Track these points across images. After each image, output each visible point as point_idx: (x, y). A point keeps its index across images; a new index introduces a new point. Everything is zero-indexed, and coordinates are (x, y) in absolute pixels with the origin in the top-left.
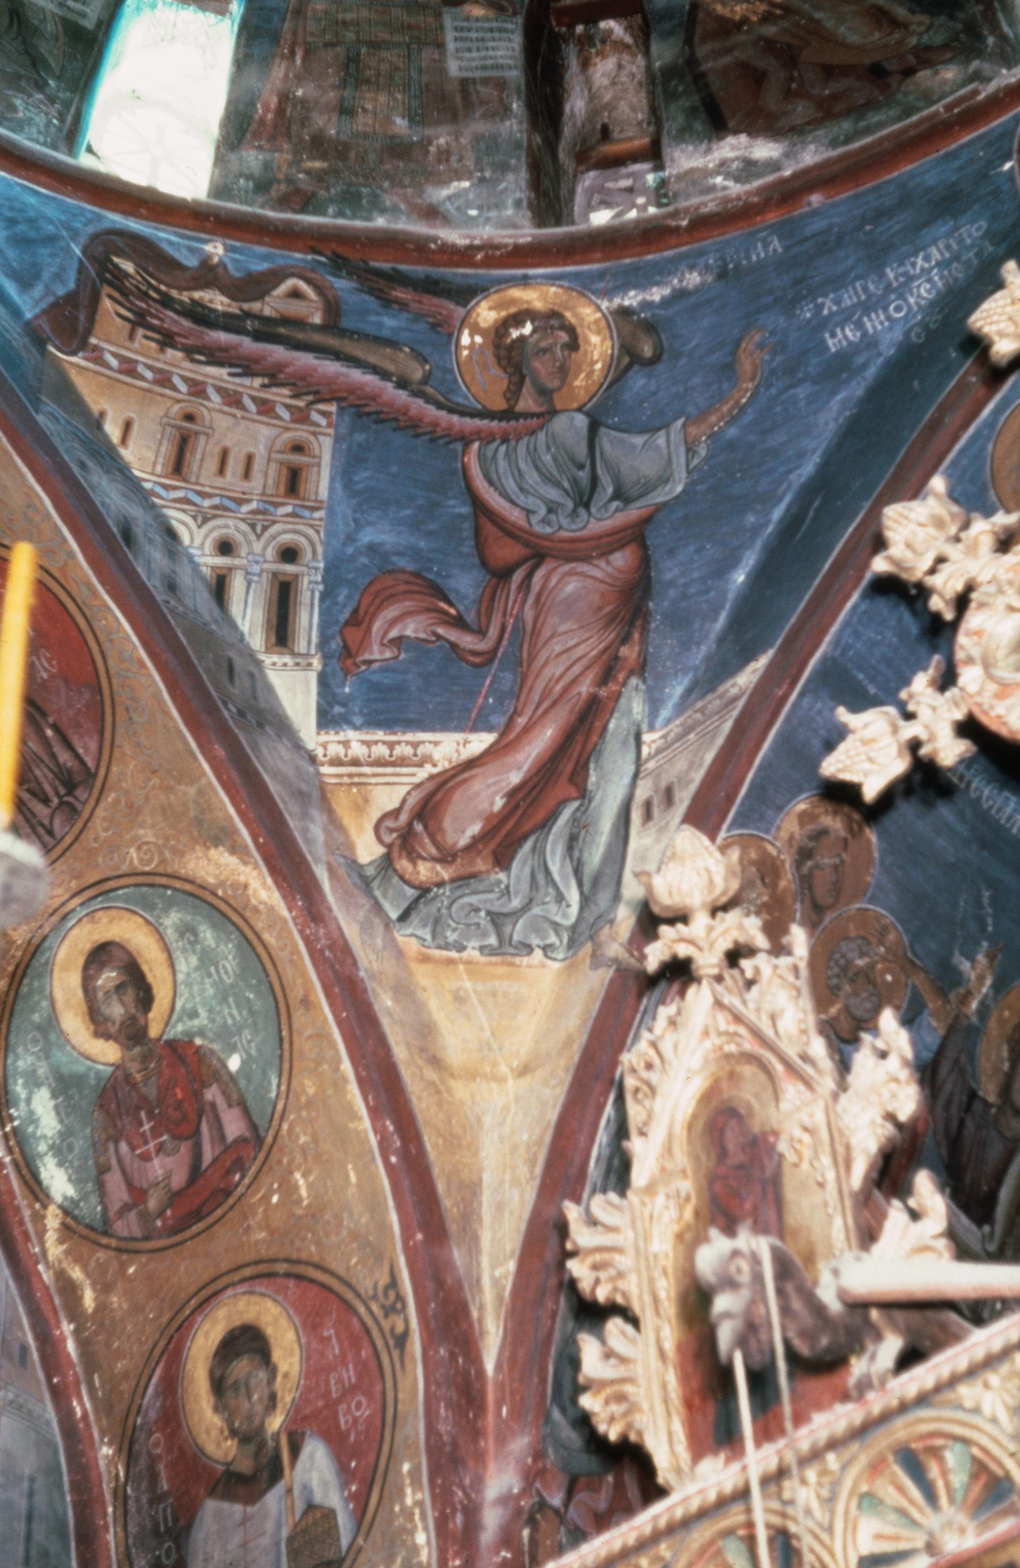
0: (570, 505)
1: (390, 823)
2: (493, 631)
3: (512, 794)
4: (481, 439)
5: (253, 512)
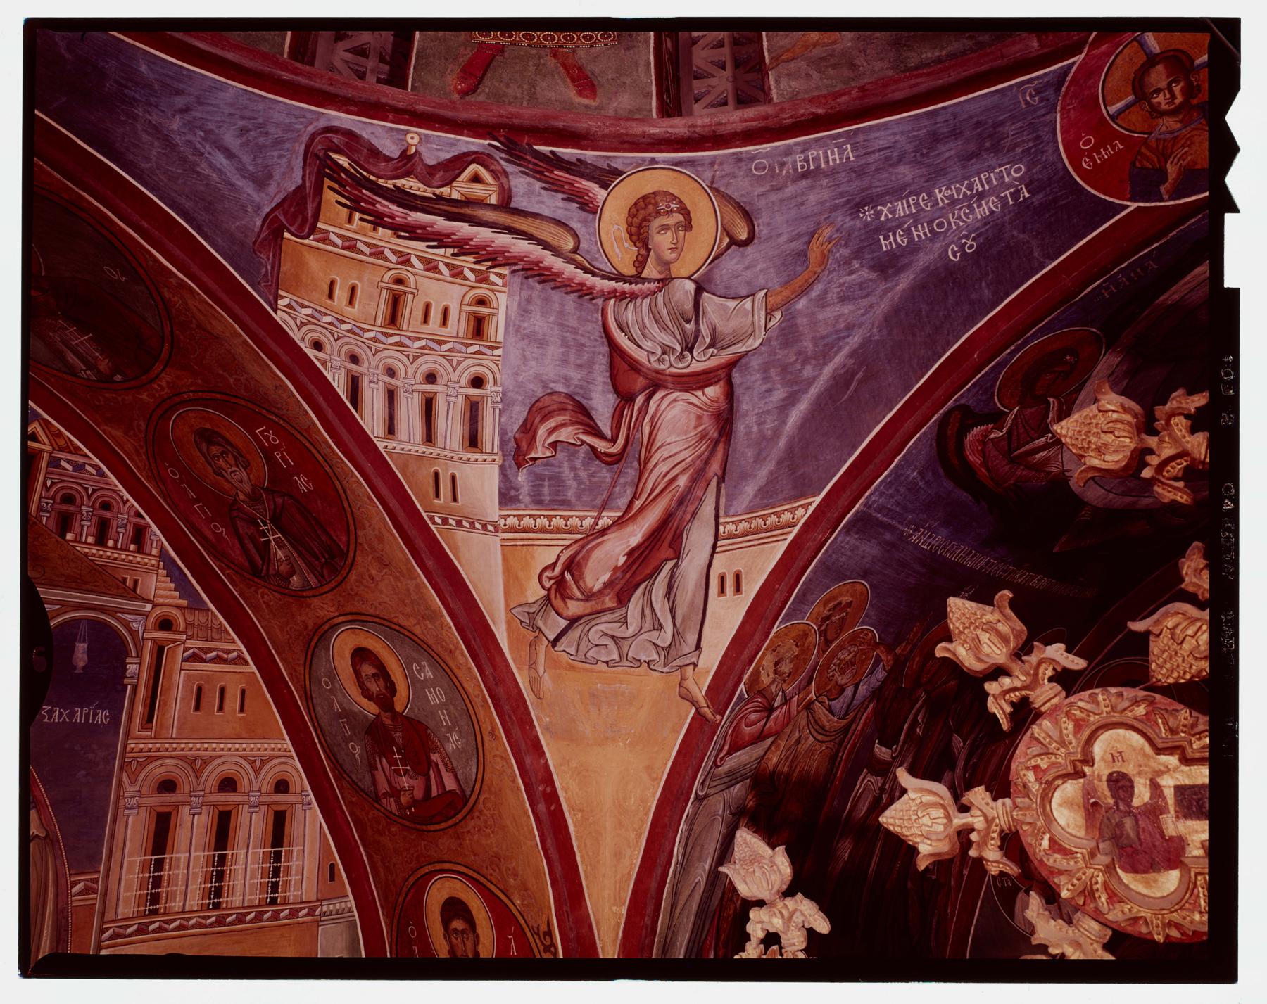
0: (679, 348)
3: (630, 554)
5: (449, 351)
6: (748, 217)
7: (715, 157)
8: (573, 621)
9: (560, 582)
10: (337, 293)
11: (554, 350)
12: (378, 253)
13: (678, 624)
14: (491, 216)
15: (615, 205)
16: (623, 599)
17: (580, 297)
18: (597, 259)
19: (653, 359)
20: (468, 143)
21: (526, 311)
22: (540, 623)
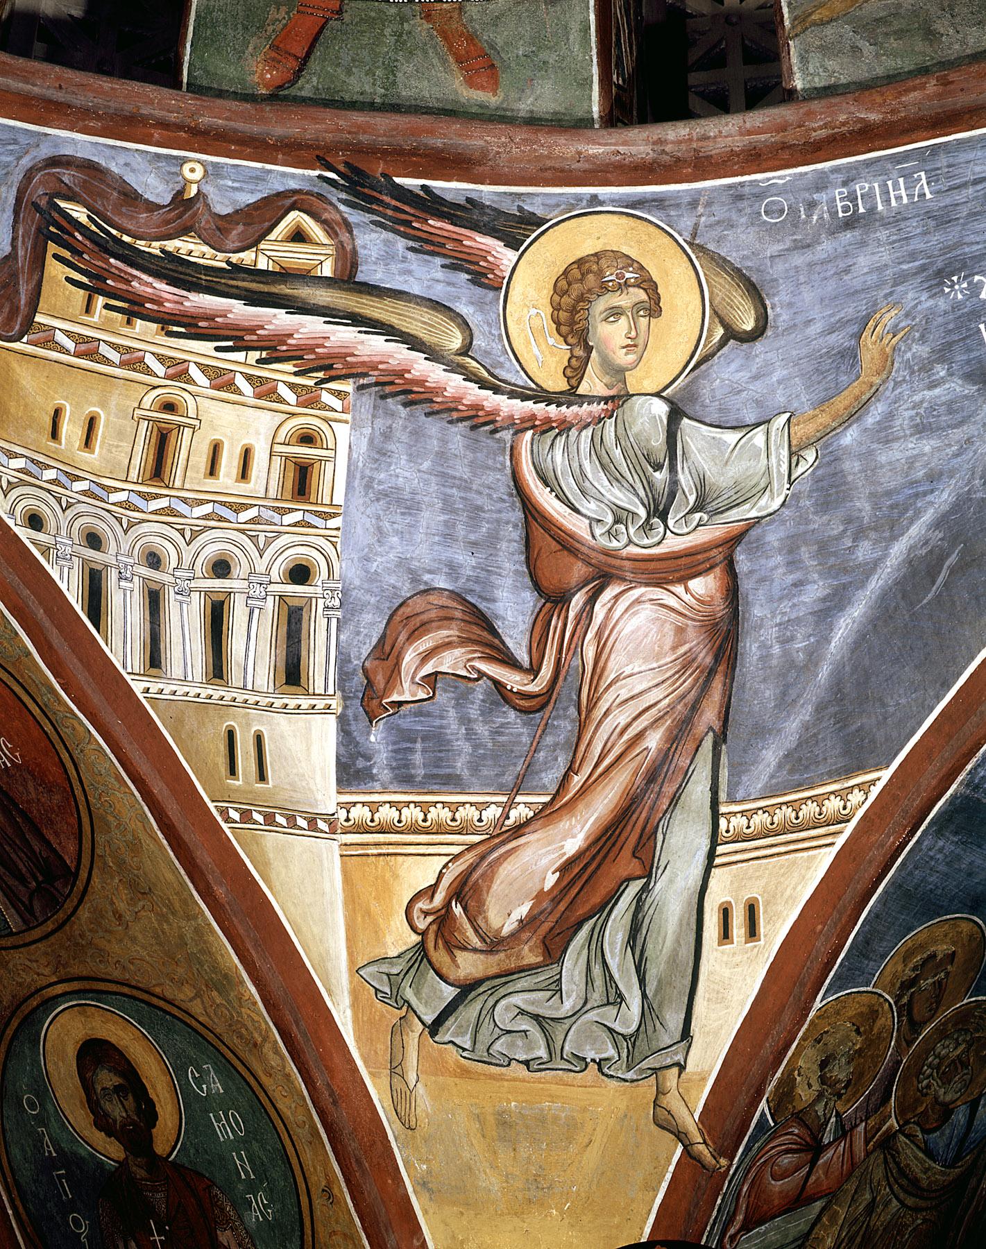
0: (642, 513)
1: (422, 905)
2: (546, 671)
3: (564, 869)
4: (533, 427)
5: (252, 521)
6: (755, 292)
7: (699, 192)
8: (467, 989)
9: (443, 918)
10: (65, 428)
11: (431, 518)
12: (134, 362)
13: (650, 992)
14: (323, 296)
15: (531, 275)
16: (553, 951)
17: (474, 428)
18: (501, 365)
19: (598, 531)
20: (284, 175)
21: (383, 453)
22: (409, 994)
